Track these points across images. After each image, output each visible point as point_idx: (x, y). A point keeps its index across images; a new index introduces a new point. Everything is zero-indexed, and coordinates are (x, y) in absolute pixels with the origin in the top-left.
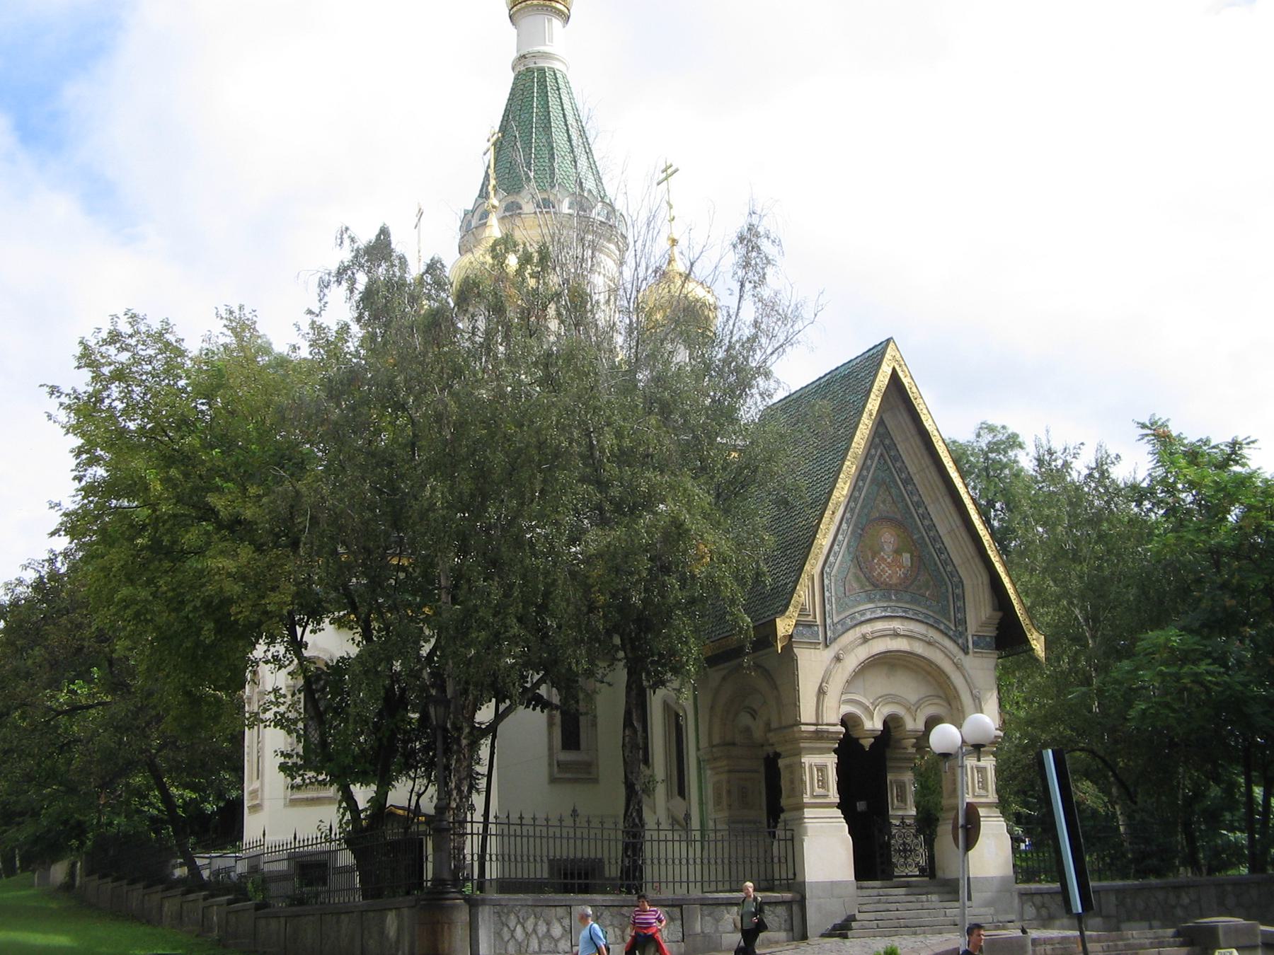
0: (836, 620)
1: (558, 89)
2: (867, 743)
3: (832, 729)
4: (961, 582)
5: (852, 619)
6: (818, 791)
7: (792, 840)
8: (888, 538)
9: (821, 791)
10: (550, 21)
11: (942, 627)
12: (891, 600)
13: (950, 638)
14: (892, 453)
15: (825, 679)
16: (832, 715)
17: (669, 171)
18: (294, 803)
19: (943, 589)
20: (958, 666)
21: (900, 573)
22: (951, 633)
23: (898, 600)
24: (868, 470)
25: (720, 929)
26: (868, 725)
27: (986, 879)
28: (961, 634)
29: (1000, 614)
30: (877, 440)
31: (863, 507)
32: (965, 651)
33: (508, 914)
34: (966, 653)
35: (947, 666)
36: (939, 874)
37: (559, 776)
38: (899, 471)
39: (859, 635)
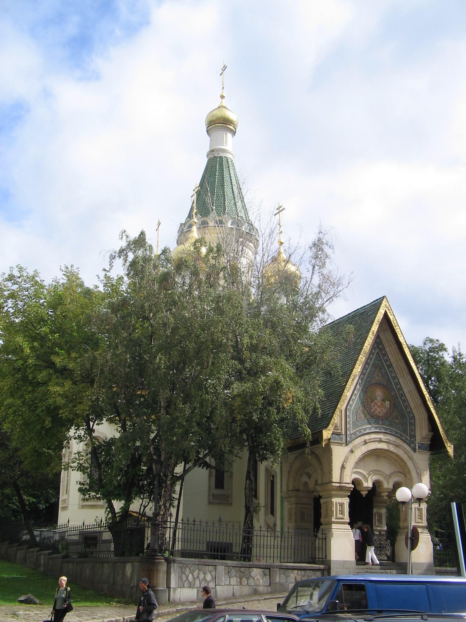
0: (352, 432)
1: (229, 167)
2: (364, 493)
3: (347, 485)
4: (414, 416)
5: (360, 432)
6: (339, 516)
7: (326, 539)
8: (379, 393)
9: (341, 516)
10: (226, 134)
11: (404, 438)
12: (379, 424)
13: (407, 444)
14: (383, 352)
15: (345, 461)
16: (348, 479)
17: (280, 209)
18: (83, 507)
19: (405, 420)
20: (411, 458)
21: (384, 411)
22: (408, 441)
23: (383, 424)
24: (371, 359)
25: (288, 581)
26: (365, 485)
27: (420, 563)
28: (413, 442)
29: (432, 434)
30: (376, 345)
31: (367, 378)
32: (414, 450)
33: (185, 568)
34: (415, 451)
35: (405, 457)
36: (397, 560)
37: (212, 501)
38: (386, 361)
39: (363, 440)
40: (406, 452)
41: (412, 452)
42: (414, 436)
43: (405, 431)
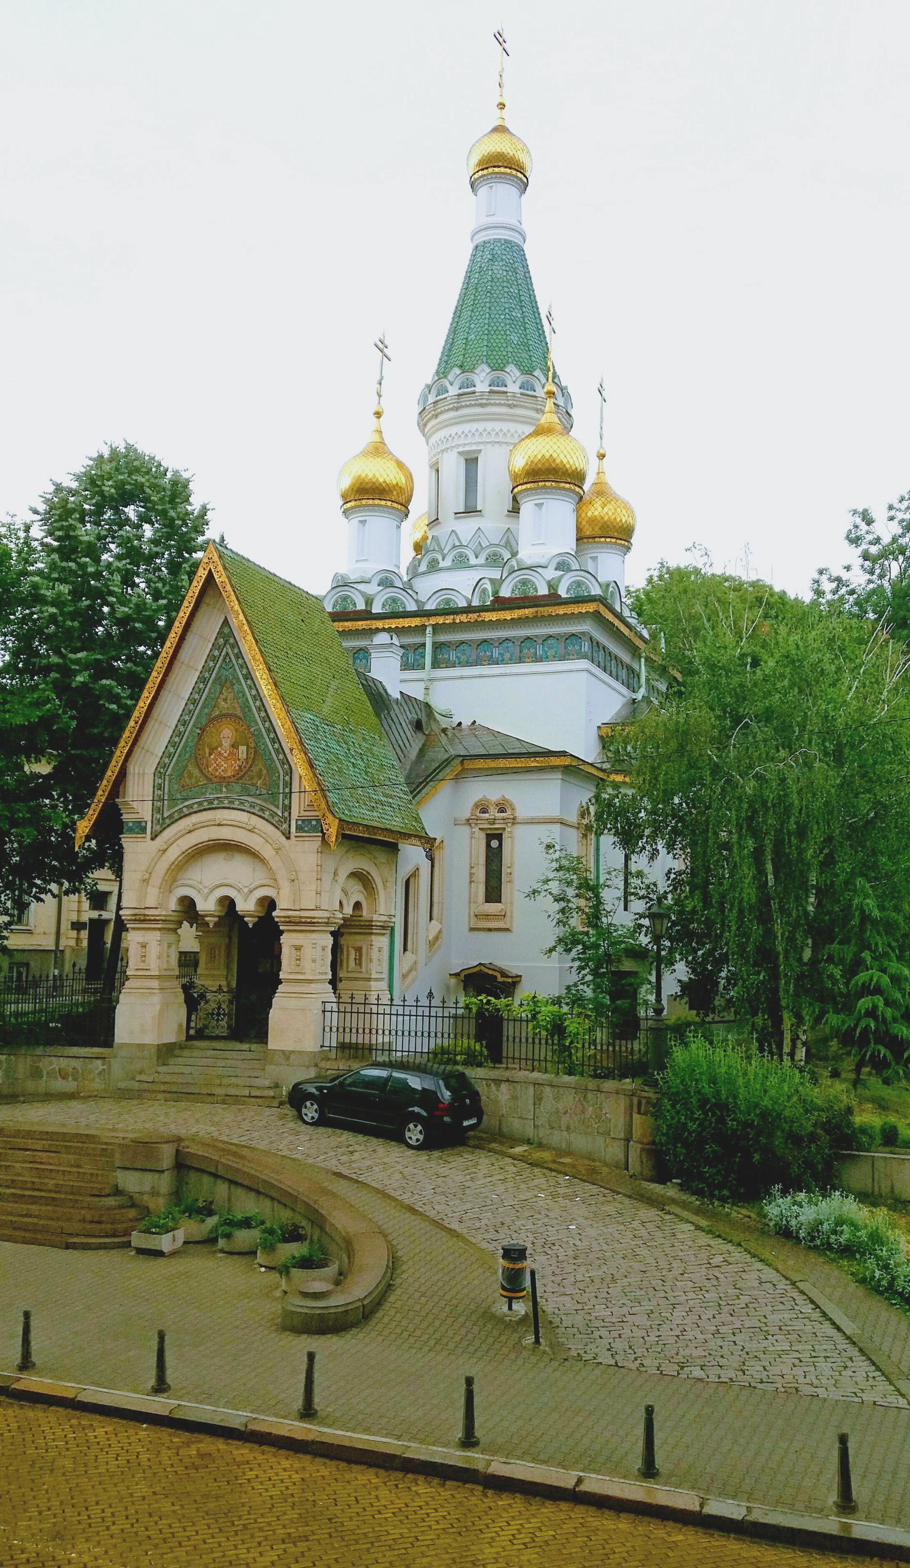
3: (147, 912)
8: (227, 734)
9: (142, 966)
12: (221, 792)
31: (203, 707)
34: (288, 838)
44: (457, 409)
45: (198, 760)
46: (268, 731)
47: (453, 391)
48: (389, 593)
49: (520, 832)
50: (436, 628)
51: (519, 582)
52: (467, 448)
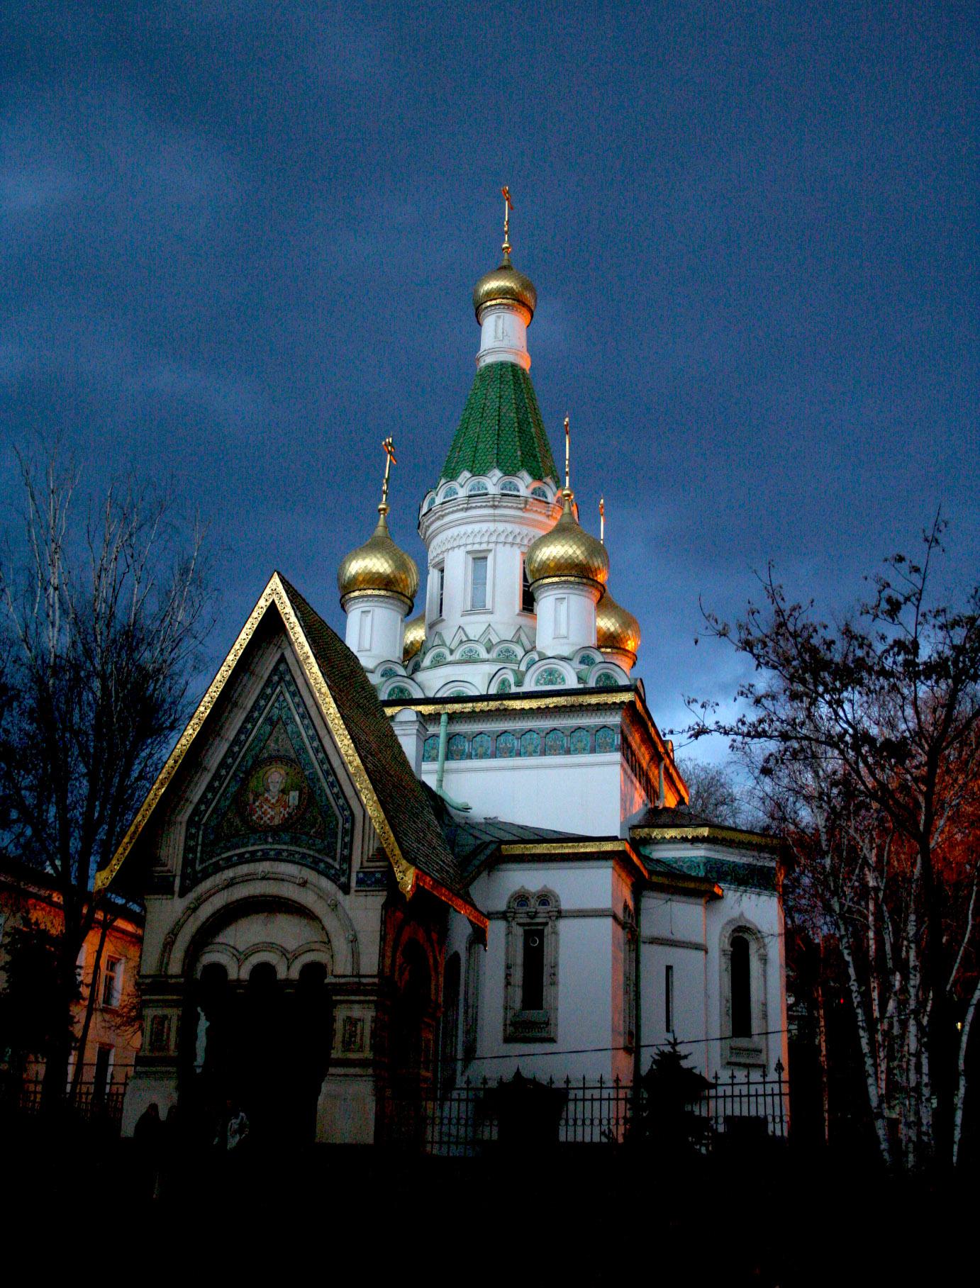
0: (198, 868)
4: (352, 814)
12: (266, 842)
30: (276, 678)
32: (346, 889)
40: (321, 895)
41: (340, 896)
42: (348, 859)
43: (330, 850)
44: (467, 509)
45: (240, 804)
46: (327, 773)
47: (462, 493)
48: (394, 682)
49: (563, 925)
50: (452, 717)
51: (545, 671)
52: (477, 547)
